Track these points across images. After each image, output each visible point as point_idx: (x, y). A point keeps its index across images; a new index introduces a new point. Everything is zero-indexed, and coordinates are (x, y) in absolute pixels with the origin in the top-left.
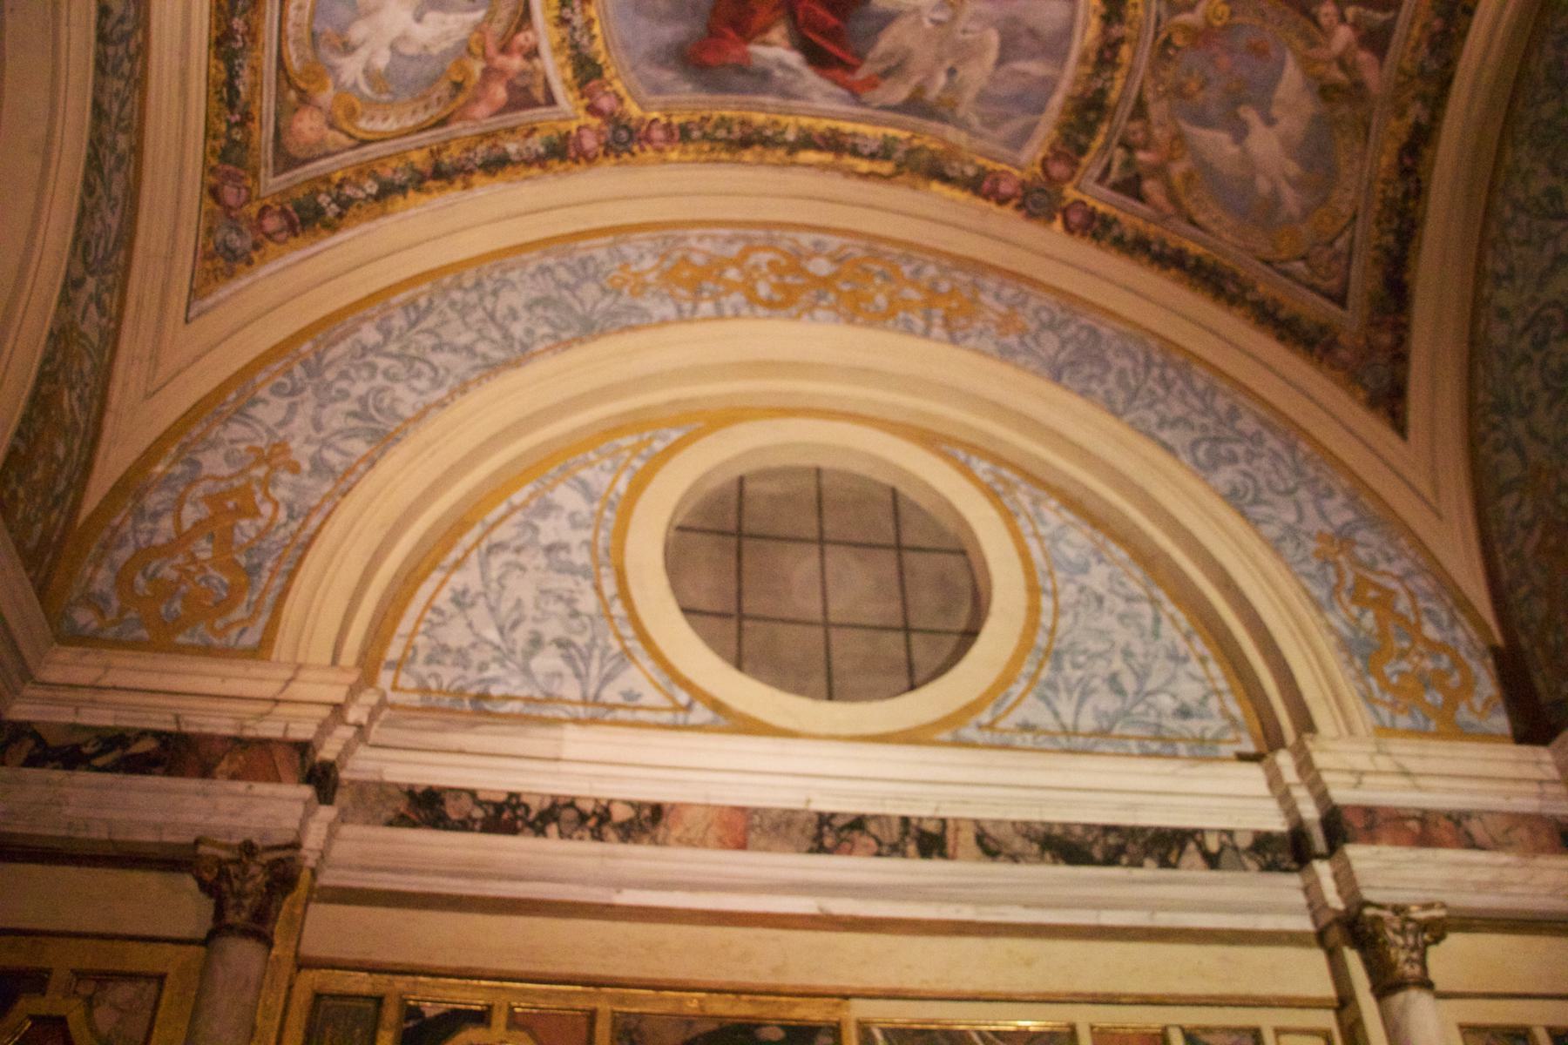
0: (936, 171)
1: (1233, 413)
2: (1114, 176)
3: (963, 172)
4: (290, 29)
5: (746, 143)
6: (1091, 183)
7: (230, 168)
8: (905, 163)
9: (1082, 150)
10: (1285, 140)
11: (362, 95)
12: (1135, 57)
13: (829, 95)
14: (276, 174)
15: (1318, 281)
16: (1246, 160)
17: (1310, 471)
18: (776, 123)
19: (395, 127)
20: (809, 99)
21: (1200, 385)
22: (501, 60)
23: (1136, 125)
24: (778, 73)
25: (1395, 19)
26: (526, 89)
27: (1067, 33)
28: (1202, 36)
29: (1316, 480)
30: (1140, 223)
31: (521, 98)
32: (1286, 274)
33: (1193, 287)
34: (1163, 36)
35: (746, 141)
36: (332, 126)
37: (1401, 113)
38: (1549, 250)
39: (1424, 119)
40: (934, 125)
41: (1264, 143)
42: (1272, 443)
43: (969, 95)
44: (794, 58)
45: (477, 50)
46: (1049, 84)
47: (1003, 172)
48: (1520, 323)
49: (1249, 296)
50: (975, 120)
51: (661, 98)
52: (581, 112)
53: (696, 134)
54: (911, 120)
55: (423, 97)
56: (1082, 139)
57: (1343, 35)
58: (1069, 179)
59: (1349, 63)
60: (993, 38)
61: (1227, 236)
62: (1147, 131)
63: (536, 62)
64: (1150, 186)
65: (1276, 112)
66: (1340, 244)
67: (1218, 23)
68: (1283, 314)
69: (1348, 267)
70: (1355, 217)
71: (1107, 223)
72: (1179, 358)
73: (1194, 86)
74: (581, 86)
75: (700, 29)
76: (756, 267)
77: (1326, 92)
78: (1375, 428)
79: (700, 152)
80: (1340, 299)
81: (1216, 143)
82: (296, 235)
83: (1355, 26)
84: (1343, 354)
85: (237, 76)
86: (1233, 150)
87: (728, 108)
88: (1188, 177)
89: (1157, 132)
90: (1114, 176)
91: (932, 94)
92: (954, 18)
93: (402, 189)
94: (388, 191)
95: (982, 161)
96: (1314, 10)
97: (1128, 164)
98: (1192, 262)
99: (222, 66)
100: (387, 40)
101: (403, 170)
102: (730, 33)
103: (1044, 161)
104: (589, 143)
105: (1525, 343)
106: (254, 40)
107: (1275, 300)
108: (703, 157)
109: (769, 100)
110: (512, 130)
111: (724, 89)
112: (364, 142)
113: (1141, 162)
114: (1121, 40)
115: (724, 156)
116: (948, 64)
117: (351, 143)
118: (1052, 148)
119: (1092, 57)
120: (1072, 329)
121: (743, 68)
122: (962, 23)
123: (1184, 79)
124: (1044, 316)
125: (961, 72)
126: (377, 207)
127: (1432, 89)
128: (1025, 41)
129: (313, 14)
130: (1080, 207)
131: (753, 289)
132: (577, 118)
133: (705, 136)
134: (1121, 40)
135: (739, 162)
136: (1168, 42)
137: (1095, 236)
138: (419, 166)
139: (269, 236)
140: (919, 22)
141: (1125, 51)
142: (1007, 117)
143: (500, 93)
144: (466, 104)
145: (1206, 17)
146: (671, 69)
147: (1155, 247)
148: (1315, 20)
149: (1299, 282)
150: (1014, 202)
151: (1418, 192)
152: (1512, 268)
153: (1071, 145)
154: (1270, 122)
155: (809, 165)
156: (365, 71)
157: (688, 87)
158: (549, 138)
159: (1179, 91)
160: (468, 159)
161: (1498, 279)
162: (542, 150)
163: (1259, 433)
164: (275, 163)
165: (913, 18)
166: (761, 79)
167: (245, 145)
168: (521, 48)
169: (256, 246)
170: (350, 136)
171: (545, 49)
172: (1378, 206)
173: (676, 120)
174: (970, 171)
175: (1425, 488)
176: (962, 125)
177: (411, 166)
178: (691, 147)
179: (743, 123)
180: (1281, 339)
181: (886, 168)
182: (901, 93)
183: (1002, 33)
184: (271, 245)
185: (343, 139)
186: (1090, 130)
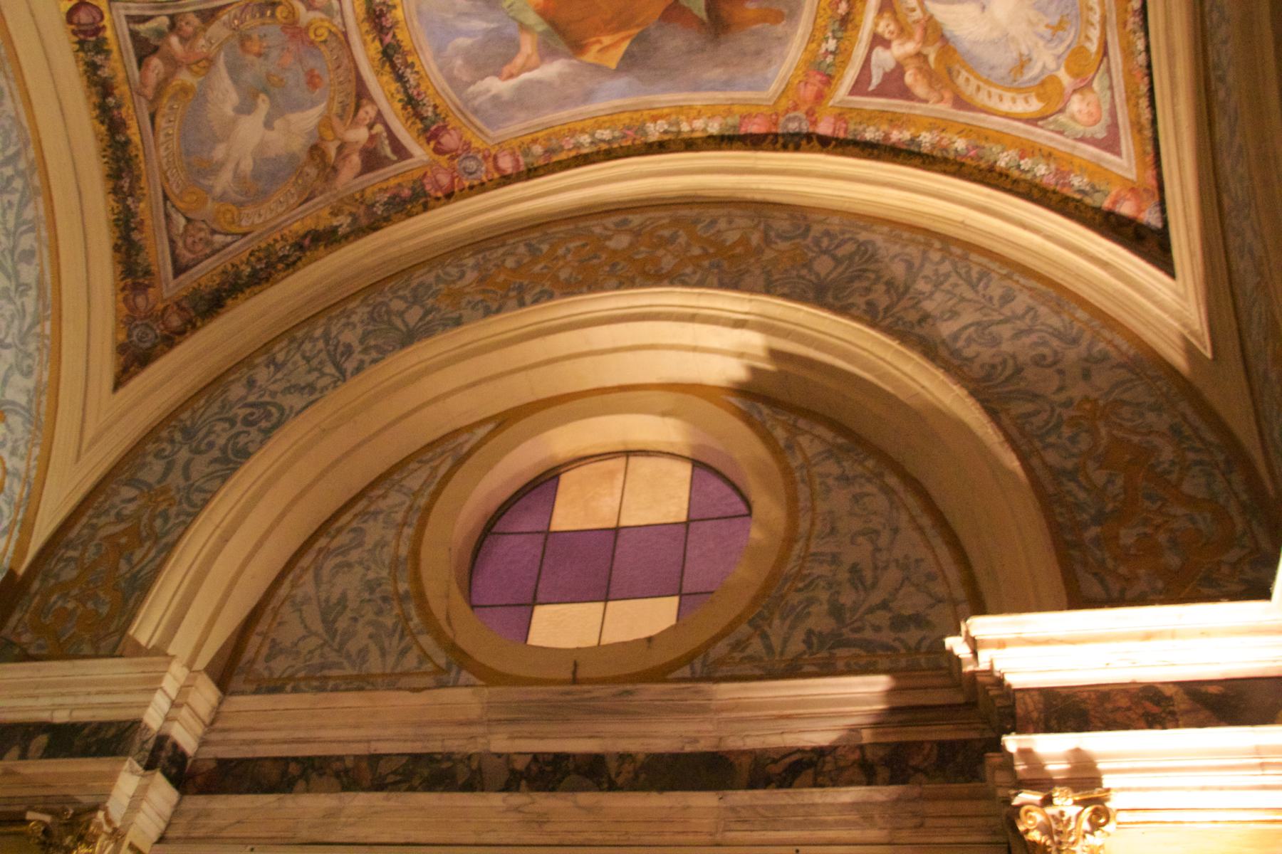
1: (28, 256)
6: (123, 12)
10: (262, 145)
15: (180, 244)
17: (32, 347)
21: (29, 213)
23: (196, 21)
25: (395, 162)
29: (29, 355)
32: (167, 216)
37: (335, 214)
38: (312, 377)
39: (341, 231)
42: (30, 301)
48: (252, 399)
49: (130, 201)
57: (360, 135)
59: (346, 151)
61: (163, 152)
62: (195, 35)
64: (155, 62)
65: (278, 123)
66: (218, 239)
68: (135, 236)
69: (207, 257)
70: (245, 235)
71: (100, 47)
72: (36, 181)
73: (256, 49)
77: (316, 151)
78: (105, 365)
80: (179, 269)
83: (372, 138)
84: (140, 301)
86: (229, 110)
88: (185, 90)
89: (202, 42)
90: (141, 28)
96: (364, 101)
97: (160, 34)
105: (243, 412)
107: (142, 222)
113: (169, 45)
123: (255, 36)
127: (364, 221)
130: (98, 19)
137: (81, 43)
145: (310, 24)
147: (111, 101)
148: (358, 108)
149: (169, 231)
151: (291, 265)
152: (284, 364)
154: (268, 124)
159: (244, 40)
161: (272, 361)
163: (28, 287)
172: (263, 245)
175: (89, 433)
180: (116, 248)
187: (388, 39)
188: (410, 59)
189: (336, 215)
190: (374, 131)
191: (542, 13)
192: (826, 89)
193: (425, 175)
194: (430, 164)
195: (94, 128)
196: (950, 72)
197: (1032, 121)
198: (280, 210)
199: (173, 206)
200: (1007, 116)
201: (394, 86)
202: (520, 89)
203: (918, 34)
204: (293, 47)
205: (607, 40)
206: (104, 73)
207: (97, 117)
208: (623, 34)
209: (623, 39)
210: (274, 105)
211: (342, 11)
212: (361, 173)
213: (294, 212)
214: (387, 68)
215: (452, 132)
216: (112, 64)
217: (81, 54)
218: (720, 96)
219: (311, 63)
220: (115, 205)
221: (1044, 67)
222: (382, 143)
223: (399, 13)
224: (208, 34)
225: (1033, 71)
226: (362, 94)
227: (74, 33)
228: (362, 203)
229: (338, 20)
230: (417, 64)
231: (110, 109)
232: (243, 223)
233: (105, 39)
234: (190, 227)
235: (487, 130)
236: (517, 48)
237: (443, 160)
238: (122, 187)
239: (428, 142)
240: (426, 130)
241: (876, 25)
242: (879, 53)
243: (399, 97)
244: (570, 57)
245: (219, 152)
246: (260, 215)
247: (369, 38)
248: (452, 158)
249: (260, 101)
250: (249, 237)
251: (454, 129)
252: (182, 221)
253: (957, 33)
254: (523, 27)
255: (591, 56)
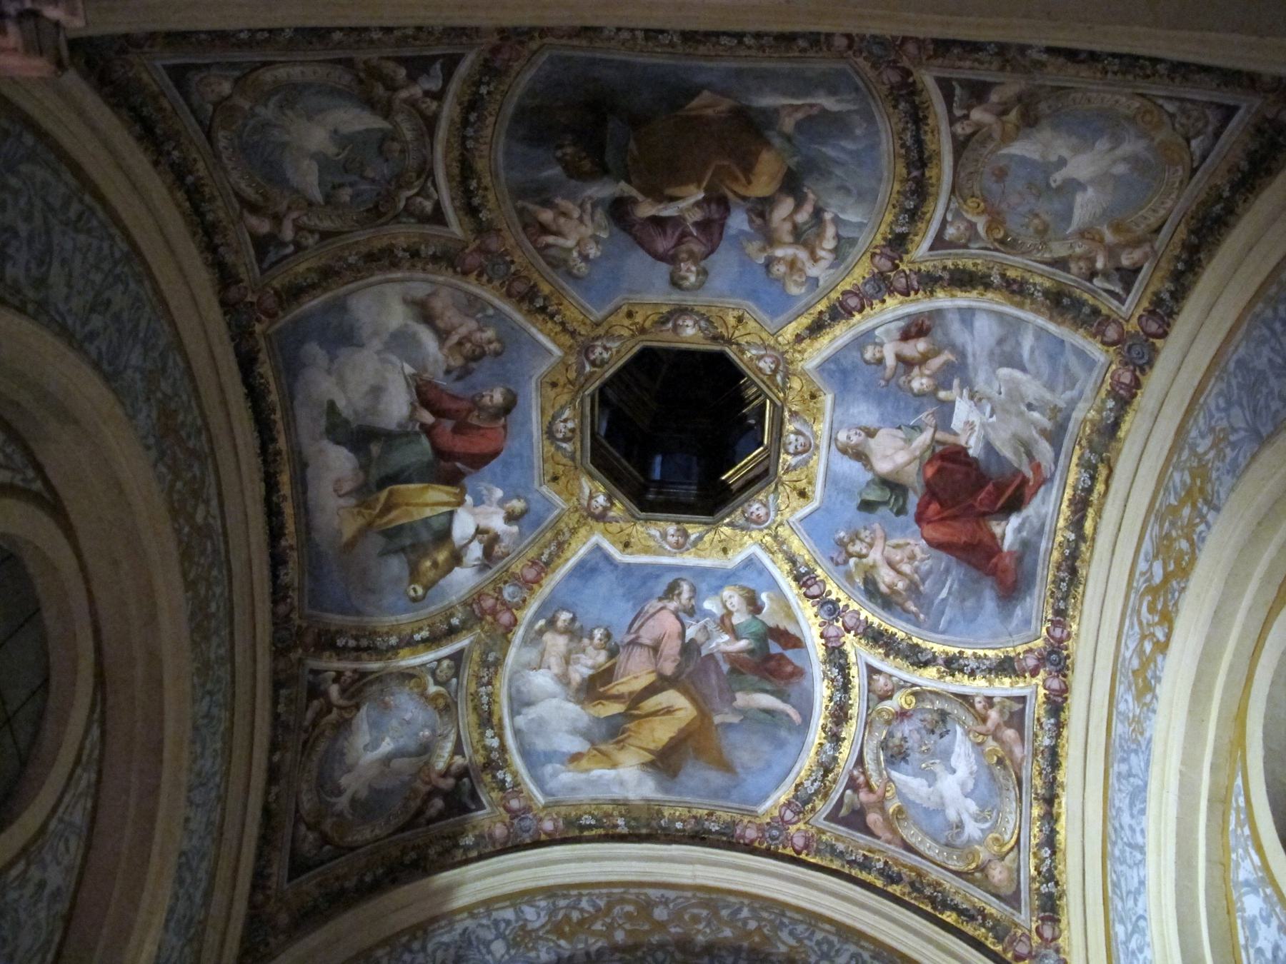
0: (1109, 431)
2: (1118, 289)
3: (1111, 410)
4: (939, 859)
5: (1073, 571)
6: (1124, 308)
7: (1007, 939)
8: (1101, 455)
9: (1096, 312)
10: (1076, 151)
11: (989, 828)
12: (1016, 266)
13: (1044, 501)
14: (1020, 912)
15: (1210, 129)
16: (1099, 181)
18: (1060, 544)
19: (1013, 816)
20: (1046, 516)
22: (990, 724)
23: (1073, 267)
24: (1024, 534)
25: (957, 80)
26: (1012, 714)
27: (1000, 316)
28: (995, 220)
30: (1159, 274)
31: (1016, 719)
32: (1204, 158)
33: (1217, 243)
34: (996, 245)
35: (1071, 570)
36: (1002, 858)
40: (1071, 425)
41: (1082, 166)
43: (1048, 396)
44: (1015, 521)
45: (980, 739)
46: (1040, 333)
47: (1112, 377)
49: (1226, 194)
50: (1069, 394)
51: (1034, 621)
52: (1034, 681)
53: (1062, 605)
54: (1067, 443)
55: (1000, 788)
56: (1086, 310)
57: (977, 115)
58: (1121, 325)
59: (1001, 108)
60: (1004, 372)
61: (1169, 204)
62: (1080, 258)
63: (995, 700)
64: (1126, 261)
65: (1053, 158)
67: (982, 205)
69: (1193, 101)
70: (1142, 95)
71: (1158, 301)
73: (1036, 221)
74: (1018, 676)
75: (988, 582)
76: (1149, 625)
77: (1030, 121)
79: (1075, 608)
80: (1228, 112)
81: (1085, 206)
82: (1059, 921)
83: (969, 108)
85: (956, 905)
86: (1090, 192)
87: (1046, 574)
88: (1117, 228)
89: (1078, 250)
90: (1118, 289)
91: (1048, 424)
92: (989, 399)
93: (1053, 832)
94: (1050, 841)
95: (1103, 393)
96: (961, 138)
97: (1106, 275)
98: (1194, 239)
99: (948, 913)
100: (962, 798)
101: (1042, 825)
102: (994, 560)
103: (1103, 343)
104: (1055, 684)
106: (940, 885)
108: (1079, 604)
109: (1043, 545)
110: (1036, 735)
111: (1034, 575)
112: (1018, 841)
114: (1003, 276)
115: (1081, 589)
116: (1024, 408)
117: (1016, 850)
118: (1094, 336)
119: (1018, 298)
120: (1234, 382)
121: (1020, 559)
122: (994, 394)
123: (1031, 230)
124: (1222, 402)
125: (1030, 399)
126: (1059, 855)
128: (1007, 348)
129: (935, 840)
130: (1144, 319)
131: (1158, 641)
132: (1037, 685)
133: (1065, 598)
134: (1003, 276)
135: (1086, 580)
136: (1002, 242)
138: (1042, 812)
139: (1054, 939)
140: (989, 425)
141: (1011, 274)
142: (1067, 369)
143: (1010, 733)
144: (1012, 761)
145: (978, 214)
146: (1015, 606)
148: (973, 134)
150: (1138, 373)
153: (1092, 320)
154: (1062, 162)
155: (1095, 529)
156: (976, 821)
157: (1028, 599)
158: (1046, 712)
160: (1046, 776)
162: (1052, 721)
164: (1013, 907)
165: (989, 429)
166: (1027, 547)
167: (997, 922)
168: (984, 707)
169: (1057, 951)
170: (1012, 849)
171: (989, 693)
172: (1130, 77)
173: (1050, 617)
174: (1111, 404)
176: (1072, 404)
177: (1041, 818)
178: (1071, 612)
179: (1058, 569)
181: (1103, 472)
182: (1044, 450)
183: (1002, 365)
184: (1060, 941)
185: (1011, 855)
186: (1078, 304)
187: (915, 173)
188: (903, 151)
189: (1039, 62)
190: (965, 112)
191: (767, 144)
192: (488, 56)
193: (929, 58)
194: (920, 64)
195: (1209, 262)
196: (361, 82)
197: (265, 64)
198: (1094, 95)
199: (1192, 160)
200: (295, 63)
201: (928, 138)
202: (807, 94)
203: (397, 104)
204: (1004, 206)
205: (710, 112)
206: (1170, 286)
207: (1200, 266)
208: (693, 113)
209: (690, 110)
210: (1047, 175)
211: (947, 209)
212: (994, 84)
213: (1083, 86)
214: (926, 154)
215: (886, 81)
216: (1159, 285)
217: (1176, 310)
218: (598, 55)
219: (995, 188)
220: (1240, 203)
221: (266, 106)
222: (961, 100)
223: (897, 187)
224: (1070, 252)
225: (272, 104)
226: (960, 146)
227: (1169, 325)
228: (1007, 61)
229: (952, 206)
230: (897, 147)
231: (1186, 262)
232: (1137, 105)
233: (1151, 303)
234: (1191, 134)
235: (850, 71)
236: (799, 125)
237: (905, 63)
238: (1223, 209)
239: (914, 82)
240: (913, 93)
241: (440, 107)
242: (434, 85)
243: (927, 128)
244: (749, 108)
245: (1121, 169)
246: (1117, 102)
247: (933, 181)
248: (895, 62)
249: (1058, 183)
250: (1140, 91)
251: (883, 83)
252: (1194, 143)
253: (358, 110)
254: (789, 139)
255: (726, 104)
